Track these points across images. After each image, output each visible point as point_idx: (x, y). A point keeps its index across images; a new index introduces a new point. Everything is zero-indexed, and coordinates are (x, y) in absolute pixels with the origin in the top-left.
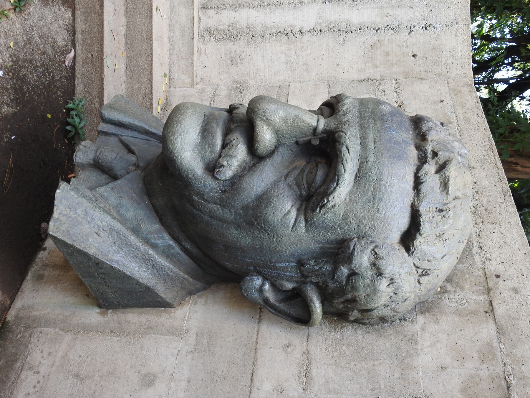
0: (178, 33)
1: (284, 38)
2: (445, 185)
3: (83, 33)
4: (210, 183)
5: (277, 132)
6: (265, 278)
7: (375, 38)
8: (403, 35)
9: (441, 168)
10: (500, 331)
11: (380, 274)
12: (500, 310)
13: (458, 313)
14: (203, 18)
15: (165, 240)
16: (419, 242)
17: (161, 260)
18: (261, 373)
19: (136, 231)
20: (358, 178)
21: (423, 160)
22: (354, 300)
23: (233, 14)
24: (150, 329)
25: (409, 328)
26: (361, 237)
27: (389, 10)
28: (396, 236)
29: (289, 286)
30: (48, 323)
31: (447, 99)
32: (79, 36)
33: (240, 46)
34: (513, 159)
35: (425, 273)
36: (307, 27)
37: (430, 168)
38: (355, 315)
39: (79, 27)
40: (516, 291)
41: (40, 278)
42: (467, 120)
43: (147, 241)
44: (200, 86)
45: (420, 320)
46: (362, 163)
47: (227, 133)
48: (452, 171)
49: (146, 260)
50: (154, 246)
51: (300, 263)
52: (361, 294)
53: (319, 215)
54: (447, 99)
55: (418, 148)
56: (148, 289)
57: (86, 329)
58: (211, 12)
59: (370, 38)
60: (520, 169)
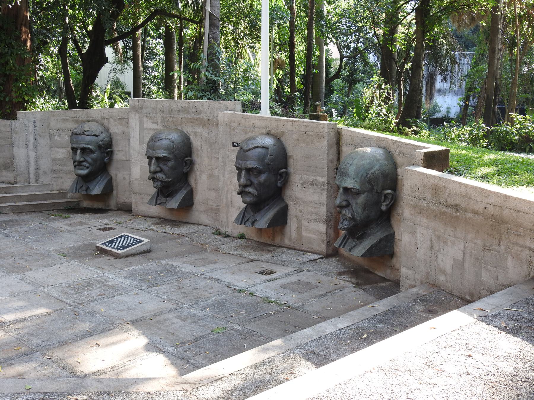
0: (38, 189)
1: (38, 160)
2: (88, 131)
3: (47, 208)
4: (90, 168)
5: (81, 157)
6: (105, 159)
7: (38, 136)
8: (37, 129)
9: (85, 131)
10: (111, 118)
11: (103, 140)
12: (107, 117)
13: (108, 124)
14: (33, 183)
15: (99, 177)
16: (97, 134)
17: (103, 178)
18: (122, 159)
19: (98, 182)
20: (88, 144)
21: (84, 134)
22: (107, 144)
23: (31, 174)
24: (116, 180)
25: (112, 133)
26: (97, 143)
27: (30, 132)
28: (97, 138)
29: (106, 155)
30: (117, 201)
31: (56, 118)
32: (48, 209)
33: (41, 172)
34: (18, 26)
35: (102, 132)
36: (35, 154)
37: (86, 133)
38: (110, 143)
39: (46, 209)
40: (104, 113)
41: (108, 206)
42: (63, 115)
43: (100, 181)
44: (53, 182)
45: (110, 131)
46: (86, 144)
47: (81, 166)
48: (86, 130)
49: (103, 180)
50: (100, 179)
51: (102, 153)
52: (106, 143)
53: (94, 150)
54: (56, 118)
55: (82, 135)
56: (108, 180)
57: (117, 192)
58: (31, 180)
59: (38, 137)
60: (24, 22)
